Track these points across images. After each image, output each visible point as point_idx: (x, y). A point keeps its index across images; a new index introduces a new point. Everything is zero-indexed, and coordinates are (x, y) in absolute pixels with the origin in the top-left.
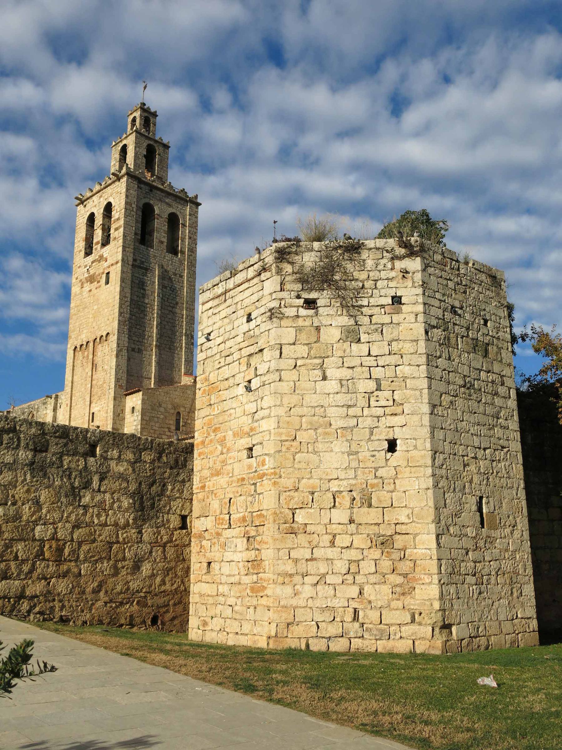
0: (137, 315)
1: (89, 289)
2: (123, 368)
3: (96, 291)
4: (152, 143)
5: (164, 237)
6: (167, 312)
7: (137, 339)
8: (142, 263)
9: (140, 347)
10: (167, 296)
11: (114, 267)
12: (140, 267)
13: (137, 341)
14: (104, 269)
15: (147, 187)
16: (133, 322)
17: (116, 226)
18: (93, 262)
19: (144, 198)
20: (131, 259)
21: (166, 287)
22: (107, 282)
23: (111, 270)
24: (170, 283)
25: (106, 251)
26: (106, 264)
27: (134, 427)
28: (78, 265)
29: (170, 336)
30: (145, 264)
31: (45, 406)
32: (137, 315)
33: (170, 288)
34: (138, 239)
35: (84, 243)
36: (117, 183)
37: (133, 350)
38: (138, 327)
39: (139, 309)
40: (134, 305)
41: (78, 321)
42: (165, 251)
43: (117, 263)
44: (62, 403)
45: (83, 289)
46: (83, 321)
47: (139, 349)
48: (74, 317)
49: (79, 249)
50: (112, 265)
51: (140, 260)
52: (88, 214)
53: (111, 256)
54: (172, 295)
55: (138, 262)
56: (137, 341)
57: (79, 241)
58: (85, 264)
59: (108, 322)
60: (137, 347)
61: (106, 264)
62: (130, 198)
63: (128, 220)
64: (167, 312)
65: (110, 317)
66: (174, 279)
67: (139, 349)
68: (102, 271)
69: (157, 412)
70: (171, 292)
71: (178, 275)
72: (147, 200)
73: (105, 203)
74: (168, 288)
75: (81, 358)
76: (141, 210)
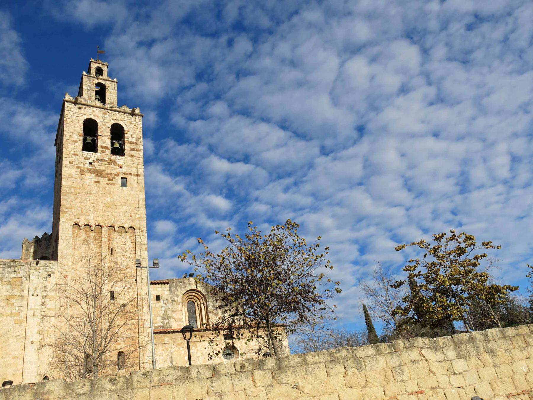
1: (96, 180)
3: (107, 186)
11: (133, 177)
14: (119, 173)
17: (133, 147)
18: (98, 160)
22: (124, 184)
23: (129, 177)
25: (118, 159)
26: (120, 170)
27: (163, 312)
28: (74, 153)
31: (13, 269)
35: (82, 138)
36: (130, 116)
41: (77, 201)
43: (138, 175)
44: (53, 273)
45: (83, 176)
46: (89, 205)
48: (68, 195)
49: (72, 139)
50: (131, 174)
52: (86, 117)
53: (127, 166)
57: (71, 132)
58: (85, 156)
59: (130, 218)
61: (120, 170)
65: (133, 215)
68: (115, 173)
73: (113, 122)
75: (84, 236)
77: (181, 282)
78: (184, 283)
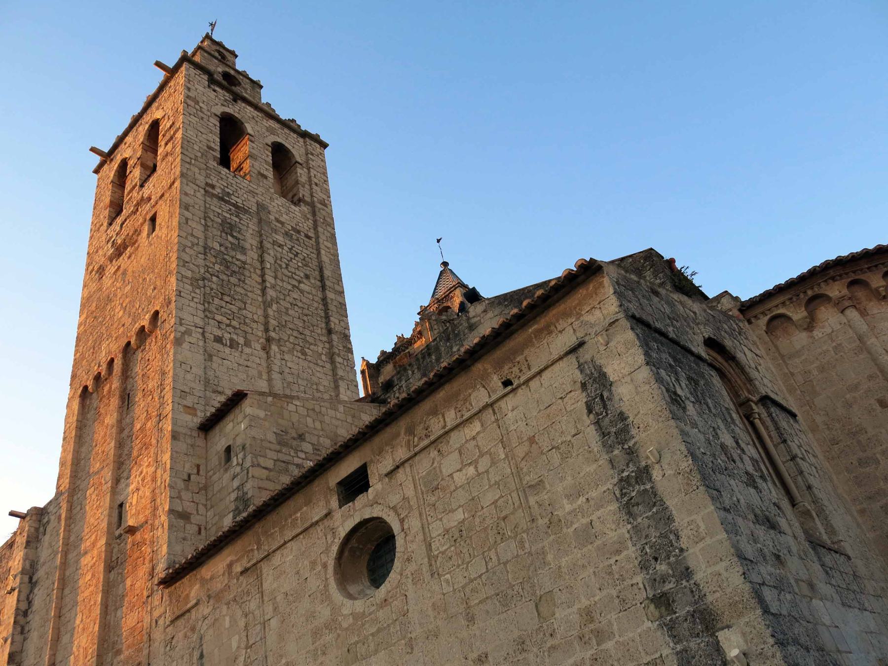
0: (225, 277)
2: (194, 370)
4: (232, 72)
6: (290, 287)
7: (228, 322)
9: (235, 337)
12: (222, 199)
13: (227, 325)
15: (227, 95)
16: (214, 286)
19: (222, 105)
21: (280, 246)
24: (287, 242)
27: (233, 496)
29: (301, 329)
32: (225, 277)
34: (215, 158)
37: (218, 340)
38: (227, 299)
39: (228, 267)
42: (272, 191)
47: (231, 340)
55: (219, 191)
56: (227, 325)
60: (227, 336)
64: (290, 287)
67: (231, 340)
69: (296, 451)
72: (227, 110)
77: (448, 339)
78: (457, 335)
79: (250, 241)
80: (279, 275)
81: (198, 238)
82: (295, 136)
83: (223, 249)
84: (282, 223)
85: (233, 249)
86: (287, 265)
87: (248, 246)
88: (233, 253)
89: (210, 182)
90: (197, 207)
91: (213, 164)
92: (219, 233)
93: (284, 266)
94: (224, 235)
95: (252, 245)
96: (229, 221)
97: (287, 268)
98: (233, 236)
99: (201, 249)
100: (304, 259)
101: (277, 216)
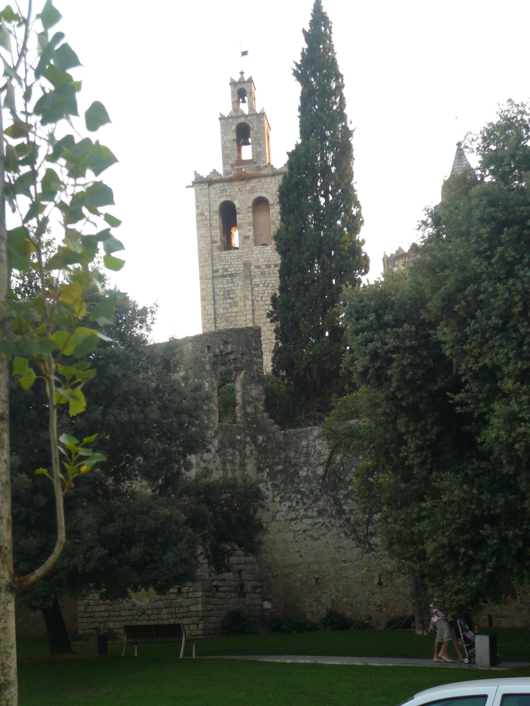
4: (242, 120)
5: (249, 230)
8: (226, 270)
10: (261, 295)
12: (224, 276)
19: (220, 197)
20: (210, 273)
21: (258, 286)
24: (263, 279)
29: (269, 337)
30: (229, 270)
33: (264, 284)
40: (221, 319)
42: (252, 245)
51: (223, 269)
54: (266, 292)
55: (221, 271)
62: (200, 208)
63: (202, 232)
66: (267, 273)
70: (264, 288)
71: (272, 266)
72: (223, 199)
74: (261, 285)
76: (218, 213)
79: (239, 295)
80: (257, 308)
81: (210, 315)
82: (268, 179)
83: (225, 311)
84: (258, 267)
85: (231, 307)
86: (261, 297)
87: (238, 299)
88: (230, 310)
89: (215, 268)
90: (209, 295)
91: (216, 253)
92: (222, 301)
93: (259, 299)
94: (225, 301)
95: (240, 297)
96: (227, 289)
97: (262, 299)
98: (230, 298)
99: (213, 320)
100: (273, 286)
101: (256, 264)
